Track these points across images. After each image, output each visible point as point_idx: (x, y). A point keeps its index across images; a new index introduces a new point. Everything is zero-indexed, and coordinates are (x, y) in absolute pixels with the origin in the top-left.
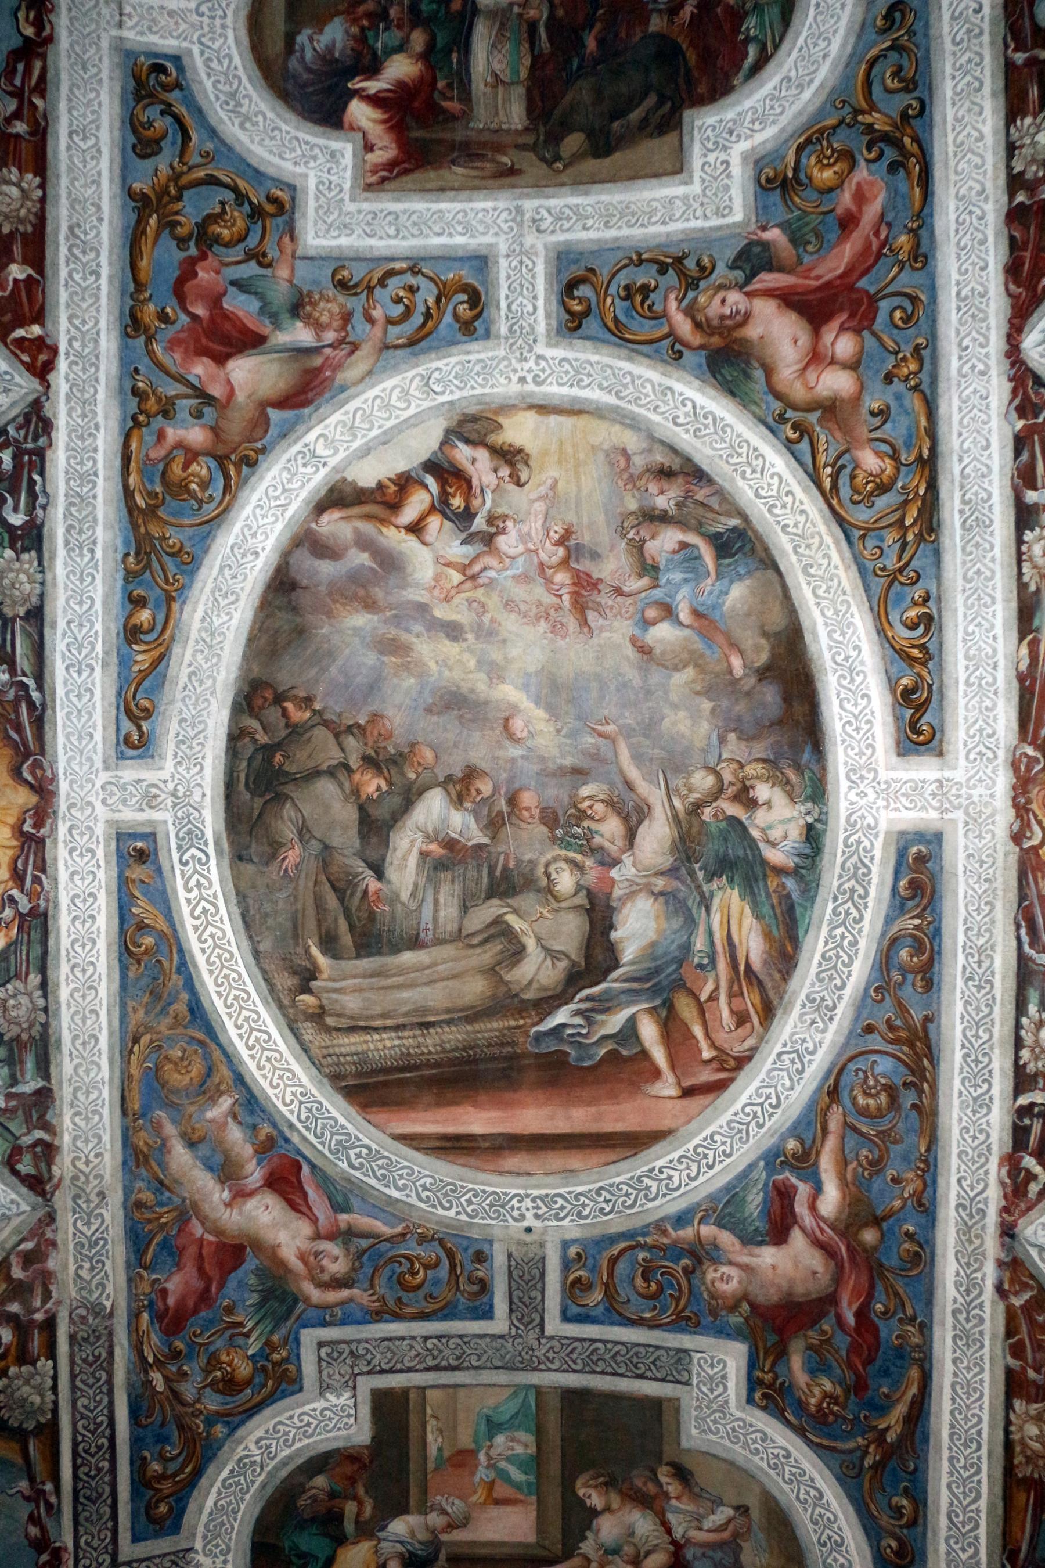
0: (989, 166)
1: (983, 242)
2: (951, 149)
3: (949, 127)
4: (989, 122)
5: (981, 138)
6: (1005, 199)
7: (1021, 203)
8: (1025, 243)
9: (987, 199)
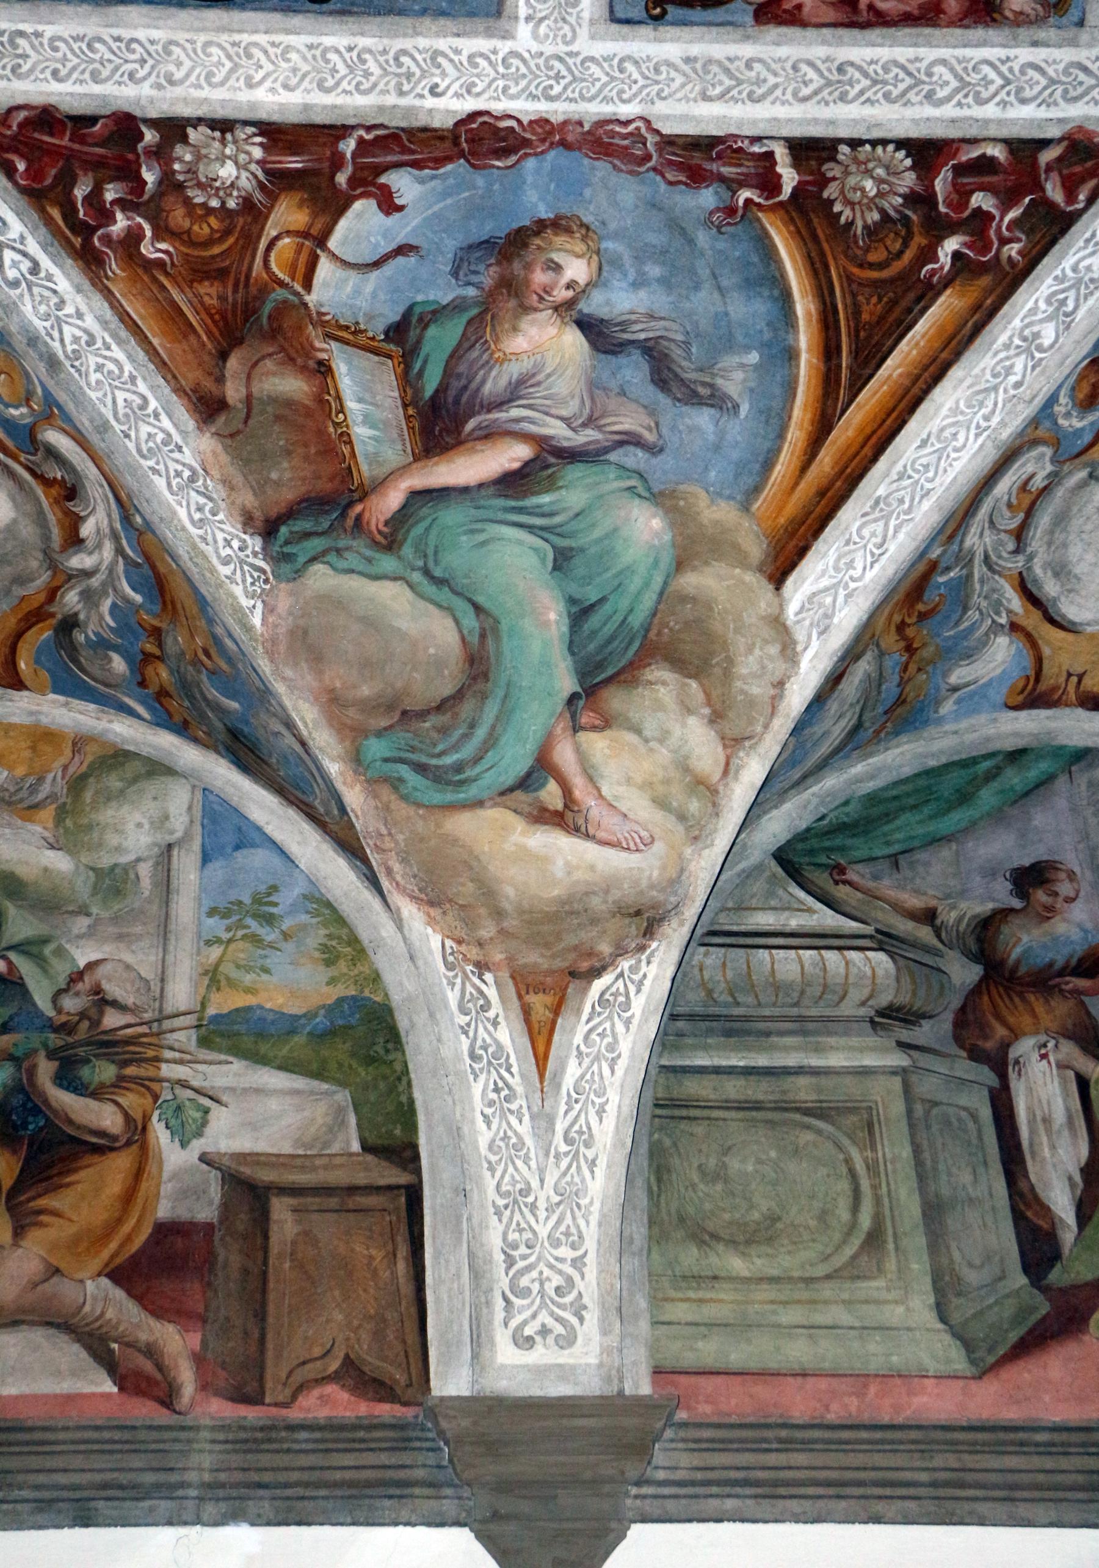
0: (206, 93)
1: (96, 77)
2: (246, 38)
3: (277, 38)
4: (270, 98)
5: (250, 85)
6: (154, 115)
7: (141, 136)
8: (82, 140)
9: (159, 87)
